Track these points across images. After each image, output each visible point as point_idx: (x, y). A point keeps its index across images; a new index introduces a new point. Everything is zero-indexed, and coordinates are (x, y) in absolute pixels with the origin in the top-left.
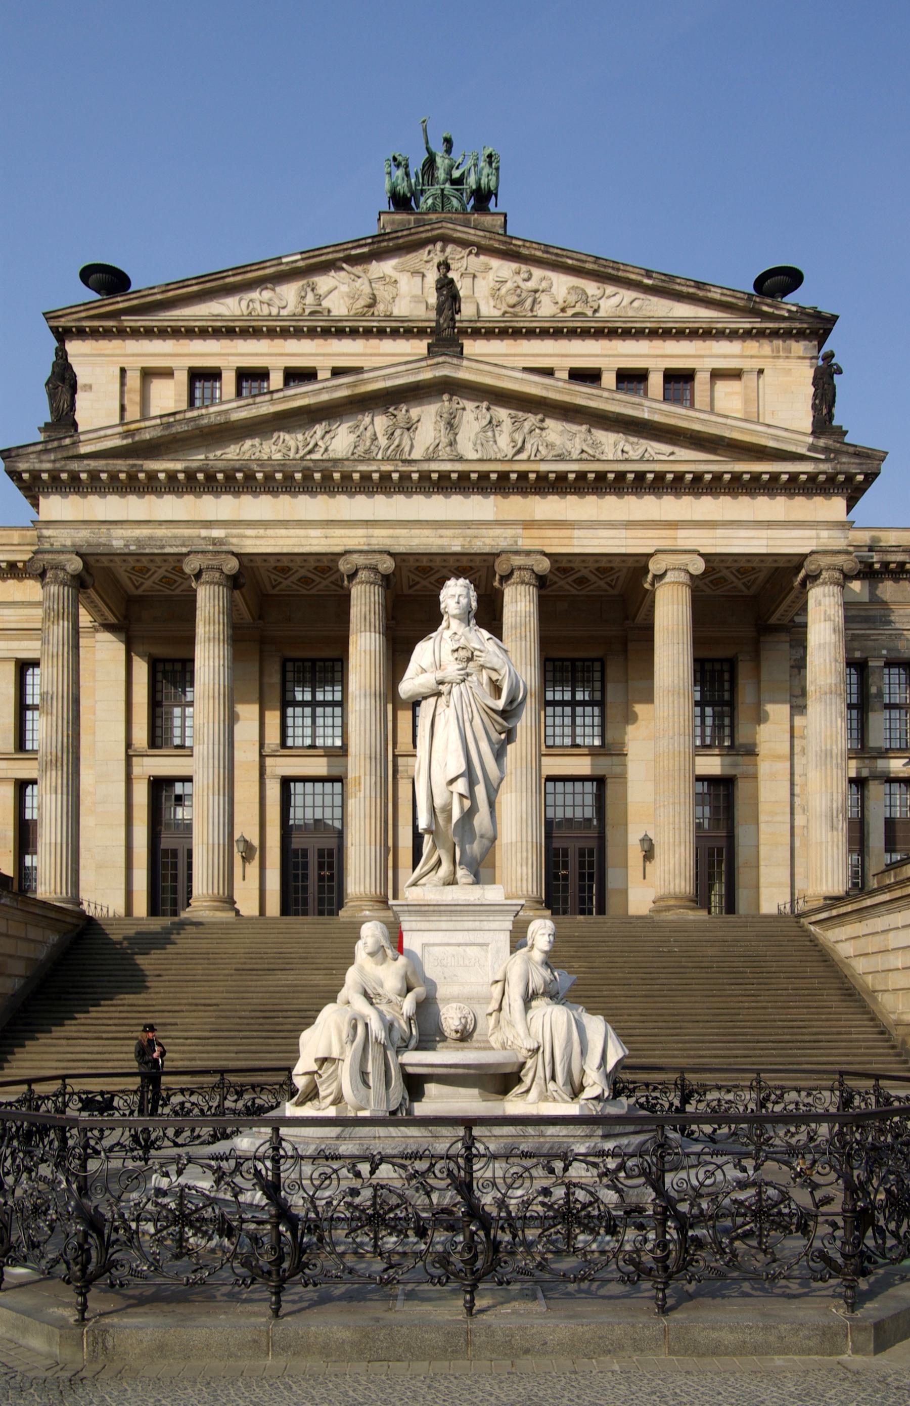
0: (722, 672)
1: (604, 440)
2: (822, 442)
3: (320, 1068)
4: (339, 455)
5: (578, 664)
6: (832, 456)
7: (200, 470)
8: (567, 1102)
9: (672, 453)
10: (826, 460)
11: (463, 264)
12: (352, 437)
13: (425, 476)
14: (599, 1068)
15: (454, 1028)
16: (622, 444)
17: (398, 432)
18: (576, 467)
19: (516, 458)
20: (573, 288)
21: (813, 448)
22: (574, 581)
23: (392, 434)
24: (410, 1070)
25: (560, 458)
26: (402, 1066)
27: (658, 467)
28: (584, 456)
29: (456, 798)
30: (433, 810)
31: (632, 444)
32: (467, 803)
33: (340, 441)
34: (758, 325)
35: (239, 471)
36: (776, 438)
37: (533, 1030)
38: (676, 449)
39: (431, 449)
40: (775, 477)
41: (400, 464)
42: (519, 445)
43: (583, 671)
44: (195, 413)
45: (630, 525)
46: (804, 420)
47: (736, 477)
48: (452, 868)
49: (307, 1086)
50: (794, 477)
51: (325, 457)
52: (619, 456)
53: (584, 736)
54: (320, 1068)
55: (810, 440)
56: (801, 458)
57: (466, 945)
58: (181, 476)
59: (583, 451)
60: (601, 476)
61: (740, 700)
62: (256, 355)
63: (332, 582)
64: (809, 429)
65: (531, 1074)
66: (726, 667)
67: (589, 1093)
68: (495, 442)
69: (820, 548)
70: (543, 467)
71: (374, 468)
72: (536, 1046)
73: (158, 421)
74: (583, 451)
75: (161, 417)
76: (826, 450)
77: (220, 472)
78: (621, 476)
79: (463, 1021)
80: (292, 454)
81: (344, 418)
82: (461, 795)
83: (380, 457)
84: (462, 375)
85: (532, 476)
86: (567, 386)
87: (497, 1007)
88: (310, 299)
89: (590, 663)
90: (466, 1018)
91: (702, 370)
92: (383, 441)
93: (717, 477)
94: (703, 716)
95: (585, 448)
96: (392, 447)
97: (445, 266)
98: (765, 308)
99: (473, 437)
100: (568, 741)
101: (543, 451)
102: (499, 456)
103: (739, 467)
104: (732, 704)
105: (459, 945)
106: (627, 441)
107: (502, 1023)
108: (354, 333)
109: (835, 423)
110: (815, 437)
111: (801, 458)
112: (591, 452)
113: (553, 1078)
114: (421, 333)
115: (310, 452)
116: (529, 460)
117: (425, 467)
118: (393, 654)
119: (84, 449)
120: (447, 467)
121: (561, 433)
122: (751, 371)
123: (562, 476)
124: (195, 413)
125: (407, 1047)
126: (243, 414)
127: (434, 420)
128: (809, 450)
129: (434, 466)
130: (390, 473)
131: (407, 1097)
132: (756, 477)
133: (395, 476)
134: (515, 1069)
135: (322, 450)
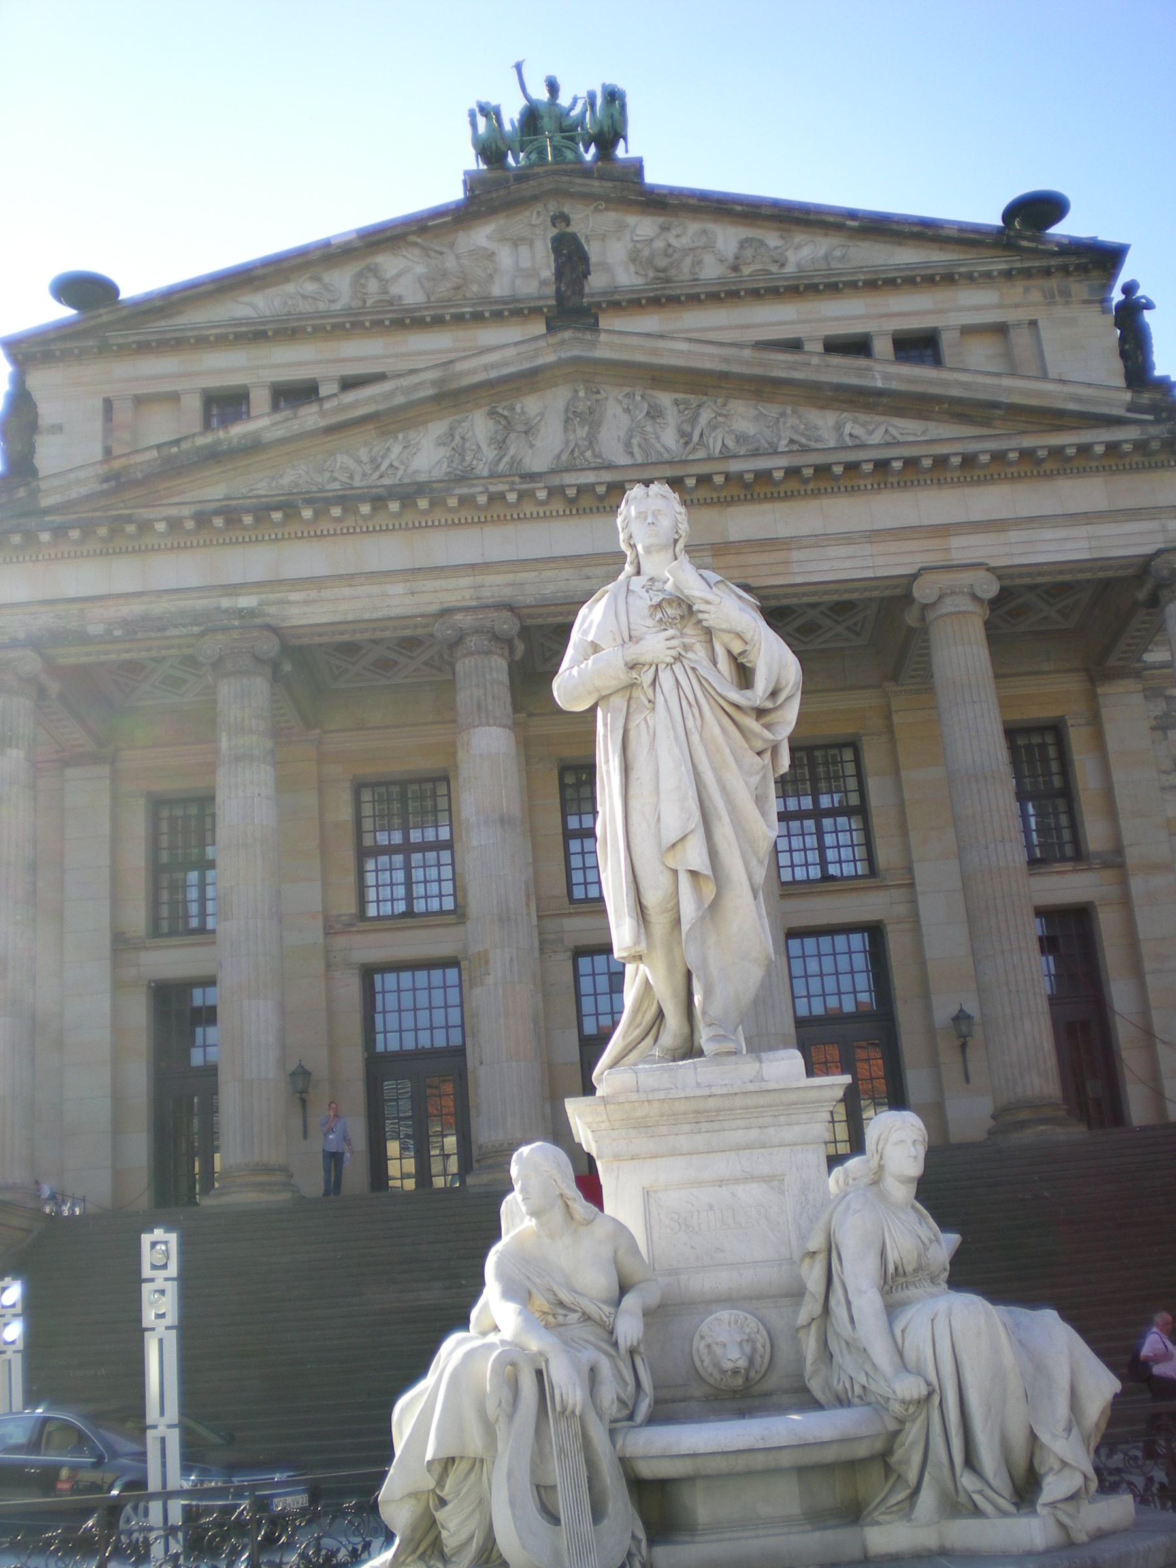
0: (1043, 746)
1: (820, 423)
2: (1145, 398)
3: (441, 1482)
4: (422, 478)
5: (818, 753)
6: (1164, 415)
7: (217, 513)
8: (1004, 1514)
9: (924, 433)
10: (1158, 421)
11: (587, 222)
12: (443, 452)
13: (555, 492)
14: (1069, 1430)
15: (728, 1365)
16: (848, 428)
17: (513, 436)
18: (784, 462)
19: (691, 457)
20: (747, 240)
21: (1132, 407)
22: (798, 630)
23: (504, 441)
24: (647, 1470)
25: (755, 454)
26: (625, 1462)
27: (908, 452)
28: (795, 447)
29: (684, 879)
30: (641, 911)
31: (864, 425)
32: (709, 891)
33: (425, 455)
34: (1018, 265)
35: (276, 508)
36: (1078, 399)
37: (910, 1355)
38: (931, 425)
39: (564, 457)
40: (1084, 450)
41: (517, 479)
42: (696, 437)
43: (826, 764)
44: (209, 439)
45: (874, 536)
46: (1112, 372)
47: (1027, 455)
48: (686, 1030)
49: (414, 1528)
50: (1112, 448)
51: (407, 480)
52: (849, 442)
53: (840, 862)
54: (441, 1482)
55: (1128, 396)
56: (1118, 421)
57: (736, 1181)
58: (190, 525)
59: (792, 441)
60: (822, 471)
61: (1080, 786)
62: (299, 364)
63: (425, 663)
64: (1121, 383)
65: (916, 1458)
66: (1049, 739)
67: (1054, 1487)
68: (658, 438)
69: (1169, 545)
70: (734, 466)
71: (480, 489)
72: (924, 1391)
73: (155, 453)
74: (792, 441)
75: (159, 447)
76: (1152, 409)
77: (248, 511)
78: (852, 467)
79: (747, 1349)
80: (357, 484)
81: (430, 425)
82: (694, 874)
83: (485, 473)
84: (600, 353)
85: (719, 480)
86: (757, 355)
87: (818, 1309)
88: (373, 286)
89: (835, 751)
90: (751, 1340)
91: (948, 328)
92: (490, 453)
93: (999, 457)
94: (1024, 816)
95: (796, 437)
96: (506, 459)
97: (561, 218)
98: (1025, 243)
99: (622, 434)
100: (815, 873)
101: (731, 444)
102: (667, 457)
103: (1028, 442)
104: (1068, 793)
105: (721, 1182)
106: (855, 421)
107: (833, 1345)
108: (438, 322)
109: (1158, 372)
110: (1134, 392)
111: (1118, 421)
112: (803, 441)
113: (970, 1462)
114: (535, 311)
115: (381, 477)
116: (710, 459)
117: (556, 481)
118: (528, 762)
119: (46, 502)
120: (589, 478)
121: (757, 418)
122: (1019, 324)
123: (763, 476)
124: (209, 439)
125: (631, 1417)
126: (279, 433)
127: (563, 418)
128: (1129, 410)
129: (570, 479)
130: (501, 496)
131: (641, 1535)
132: (1056, 452)
133: (512, 497)
134: (879, 1445)
135: (400, 473)
